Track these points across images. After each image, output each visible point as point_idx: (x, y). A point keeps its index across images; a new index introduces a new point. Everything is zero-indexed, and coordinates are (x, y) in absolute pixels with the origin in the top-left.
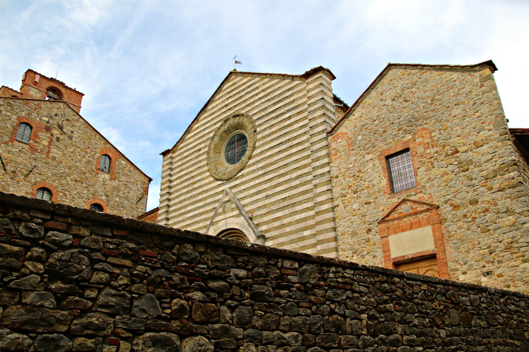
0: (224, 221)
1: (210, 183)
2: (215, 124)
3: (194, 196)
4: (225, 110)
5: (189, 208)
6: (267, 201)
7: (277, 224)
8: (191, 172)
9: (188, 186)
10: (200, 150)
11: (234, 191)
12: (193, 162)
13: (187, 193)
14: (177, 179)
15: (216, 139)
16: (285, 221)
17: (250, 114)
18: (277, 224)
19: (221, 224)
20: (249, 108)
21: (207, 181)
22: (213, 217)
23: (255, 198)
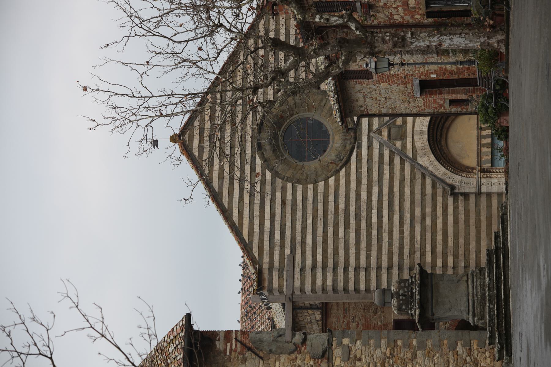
0: (415, 137)
1: (348, 175)
3: (358, 208)
5: (374, 219)
8: (315, 218)
9: (336, 225)
10: (284, 202)
12: (299, 214)
19: (418, 144)
21: (342, 182)
22: (402, 162)
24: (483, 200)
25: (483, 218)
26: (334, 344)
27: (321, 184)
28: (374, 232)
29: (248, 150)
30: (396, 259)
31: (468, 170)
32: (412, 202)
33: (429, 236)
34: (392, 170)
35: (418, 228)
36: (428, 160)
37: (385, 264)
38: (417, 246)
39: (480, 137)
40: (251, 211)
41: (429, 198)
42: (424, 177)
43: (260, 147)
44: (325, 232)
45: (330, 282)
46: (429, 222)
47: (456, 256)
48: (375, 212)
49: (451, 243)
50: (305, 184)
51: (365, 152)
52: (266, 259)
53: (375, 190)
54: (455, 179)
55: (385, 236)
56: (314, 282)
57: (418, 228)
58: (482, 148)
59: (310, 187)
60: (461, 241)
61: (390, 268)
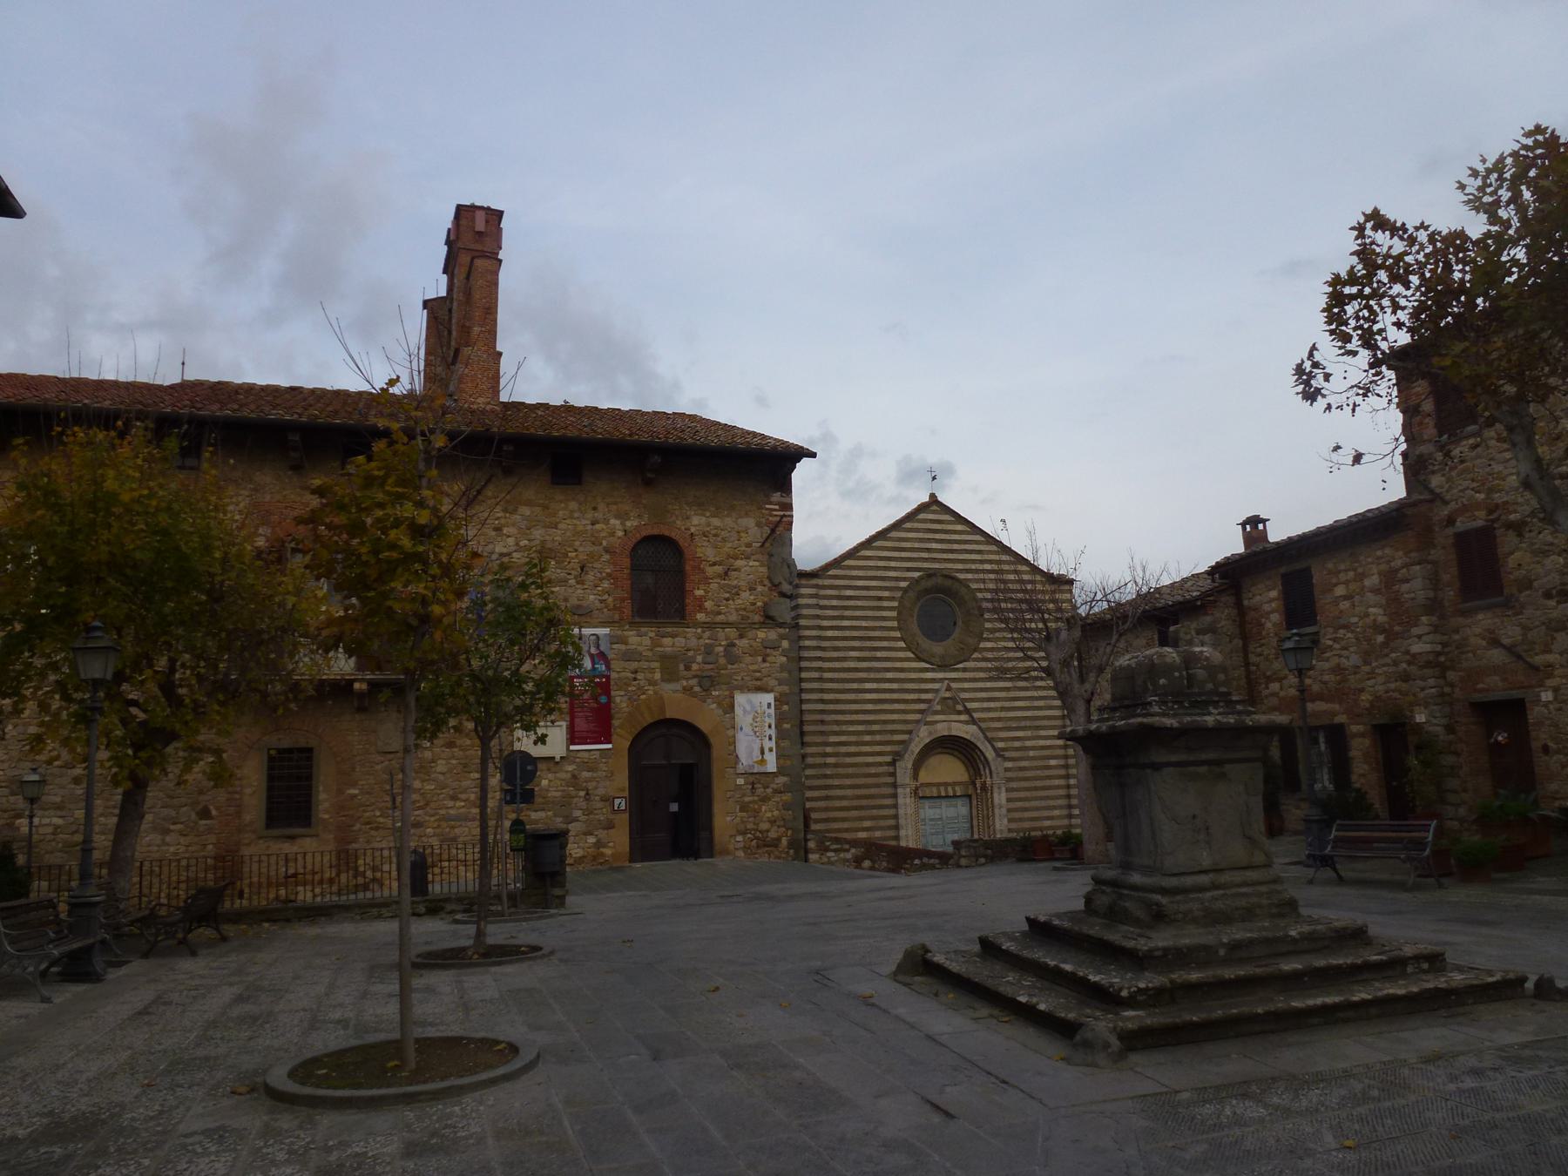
2: (908, 569)
4: (925, 555)
5: (868, 686)
6: (1003, 714)
7: (1017, 744)
8: (866, 628)
10: (880, 599)
11: (954, 685)
12: (870, 613)
13: (859, 659)
14: (832, 628)
15: (911, 594)
16: (1028, 743)
17: (974, 586)
18: (1017, 744)
19: (939, 726)
20: (970, 576)
21: (901, 654)
22: (921, 712)
23: (986, 705)
24: (890, 791)
25: (873, 791)
26: (781, 631)
27: (898, 634)
28: (855, 686)
29: (926, 565)
30: (831, 707)
31: (915, 776)
32: (885, 722)
33: (853, 738)
34: (914, 701)
35: (860, 728)
36: (924, 736)
37: (826, 696)
38: (844, 728)
39: (946, 784)
40: (871, 568)
41: (888, 737)
42: (910, 732)
43: (930, 574)
44: (854, 638)
45: (807, 643)
46: (867, 738)
47: (836, 765)
48: (875, 686)
49: (848, 760)
50: (898, 619)
51: (929, 675)
52: (827, 582)
53: (895, 686)
54: (906, 764)
55: (852, 696)
56: (808, 628)
57: (860, 728)
59: (895, 624)
60: (850, 770)
61: (822, 701)
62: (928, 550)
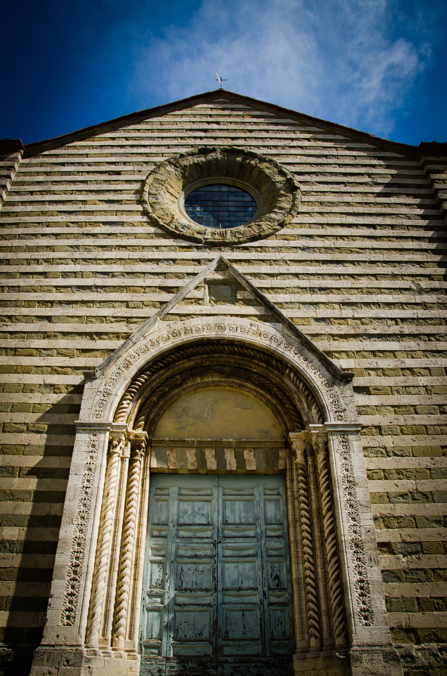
0: (212, 317)
4: (202, 134)
8: (84, 202)
10: (118, 173)
20: (274, 151)
58: (194, 451)
62: (205, 131)
